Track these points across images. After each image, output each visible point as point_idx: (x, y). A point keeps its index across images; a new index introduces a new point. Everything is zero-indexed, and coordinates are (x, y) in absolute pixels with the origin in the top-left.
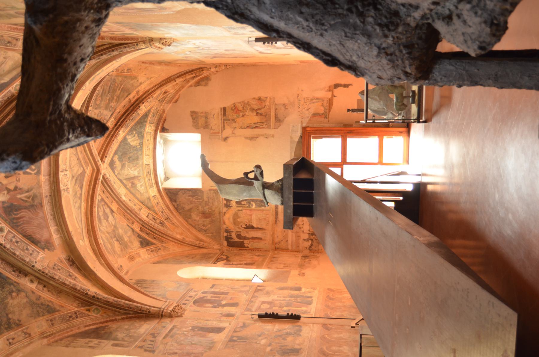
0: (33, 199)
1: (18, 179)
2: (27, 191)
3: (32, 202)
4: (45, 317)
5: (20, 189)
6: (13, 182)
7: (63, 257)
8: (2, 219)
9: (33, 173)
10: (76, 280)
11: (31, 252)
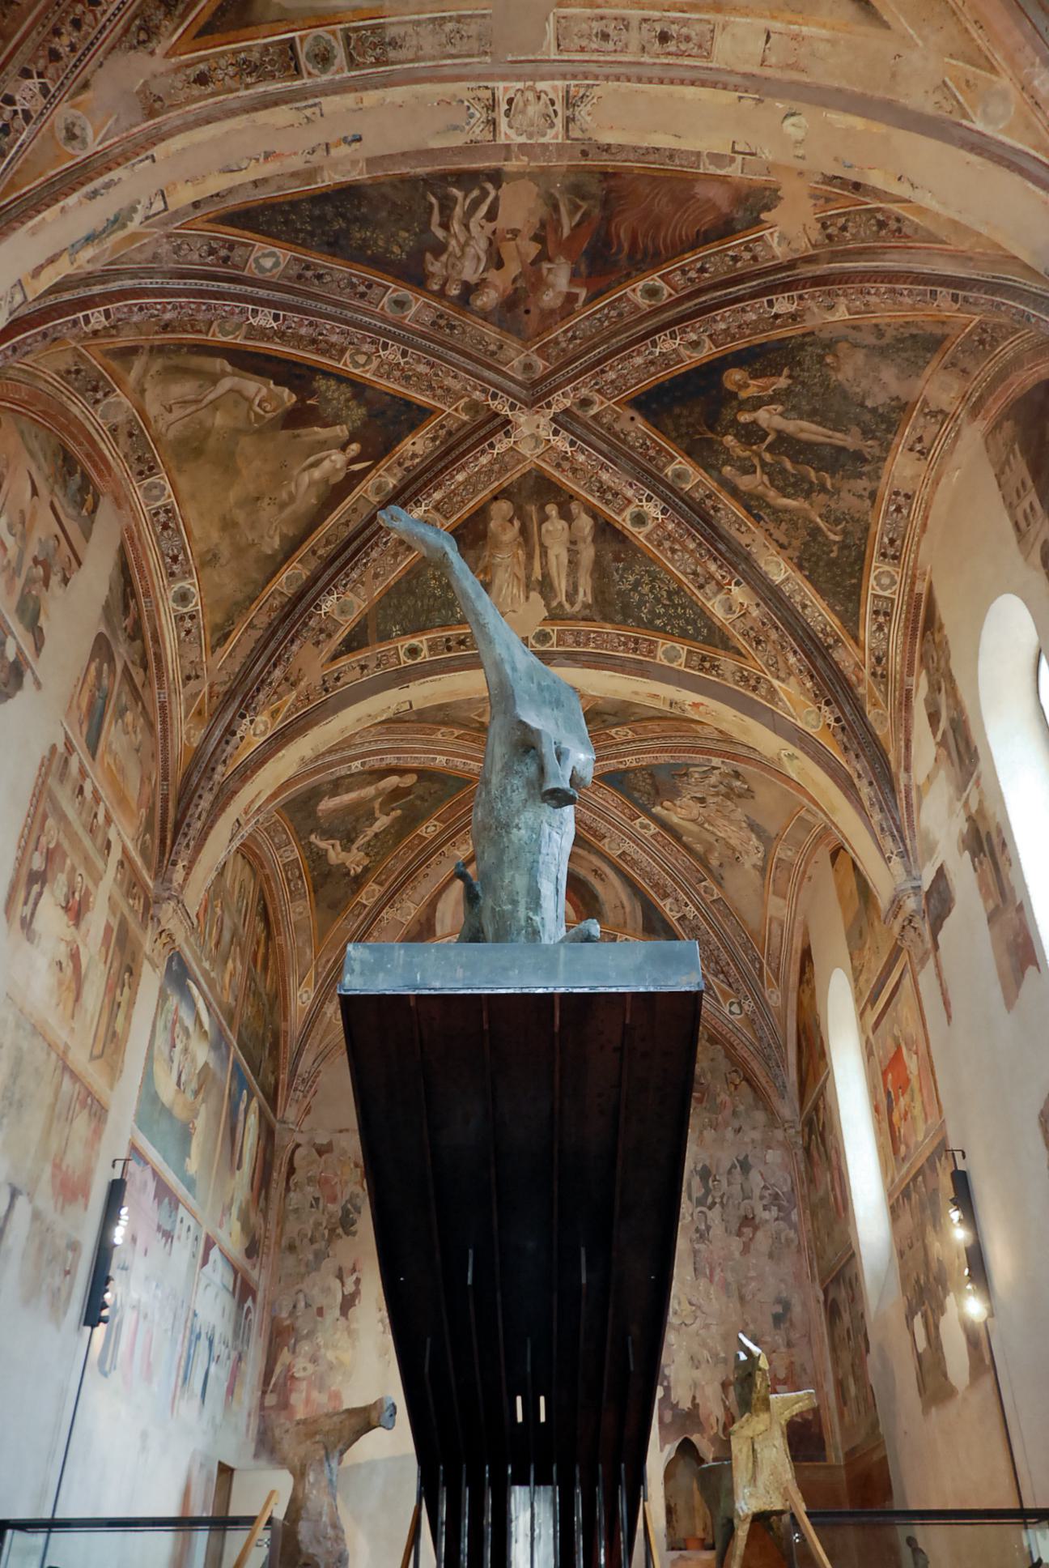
0: (583, 198)
1: (509, 236)
2: (556, 208)
3: (592, 202)
4: (934, 363)
5: (543, 225)
6: (517, 246)
7: (817, 183)
8: (620, 283)
9: (493, 193)
10: (906, 230)
11: (747, 255)
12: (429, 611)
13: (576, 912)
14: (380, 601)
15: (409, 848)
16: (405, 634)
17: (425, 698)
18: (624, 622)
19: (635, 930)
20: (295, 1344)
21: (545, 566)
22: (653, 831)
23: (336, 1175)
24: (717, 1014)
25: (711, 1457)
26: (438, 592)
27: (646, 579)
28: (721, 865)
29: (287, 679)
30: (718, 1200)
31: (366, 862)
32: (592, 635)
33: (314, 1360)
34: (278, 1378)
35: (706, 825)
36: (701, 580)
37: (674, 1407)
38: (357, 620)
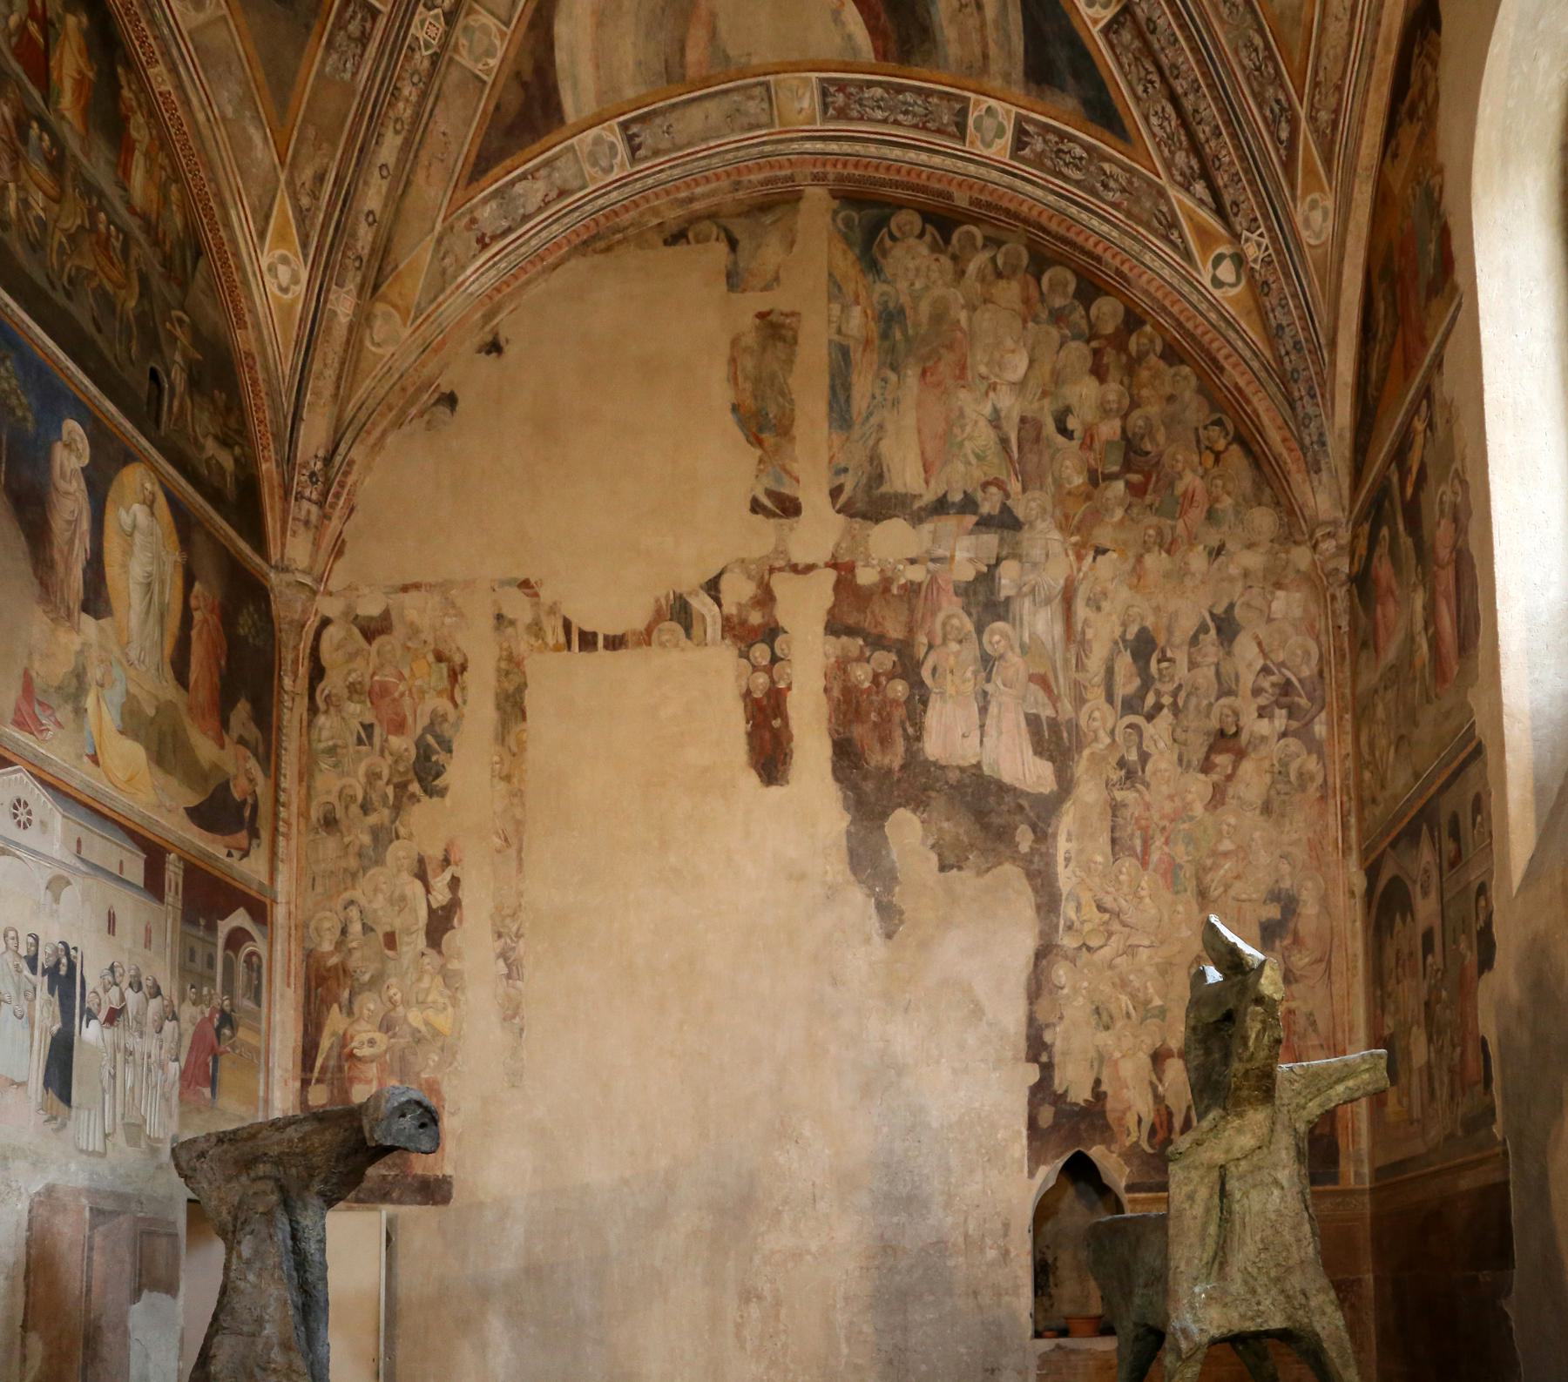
20: (350, 1002)
23: (401, 677)
25: (1123, 1184)
30: (1166, 700)
33: (387, 1026)
34: (327, 1058)
37: (1059, 1099)
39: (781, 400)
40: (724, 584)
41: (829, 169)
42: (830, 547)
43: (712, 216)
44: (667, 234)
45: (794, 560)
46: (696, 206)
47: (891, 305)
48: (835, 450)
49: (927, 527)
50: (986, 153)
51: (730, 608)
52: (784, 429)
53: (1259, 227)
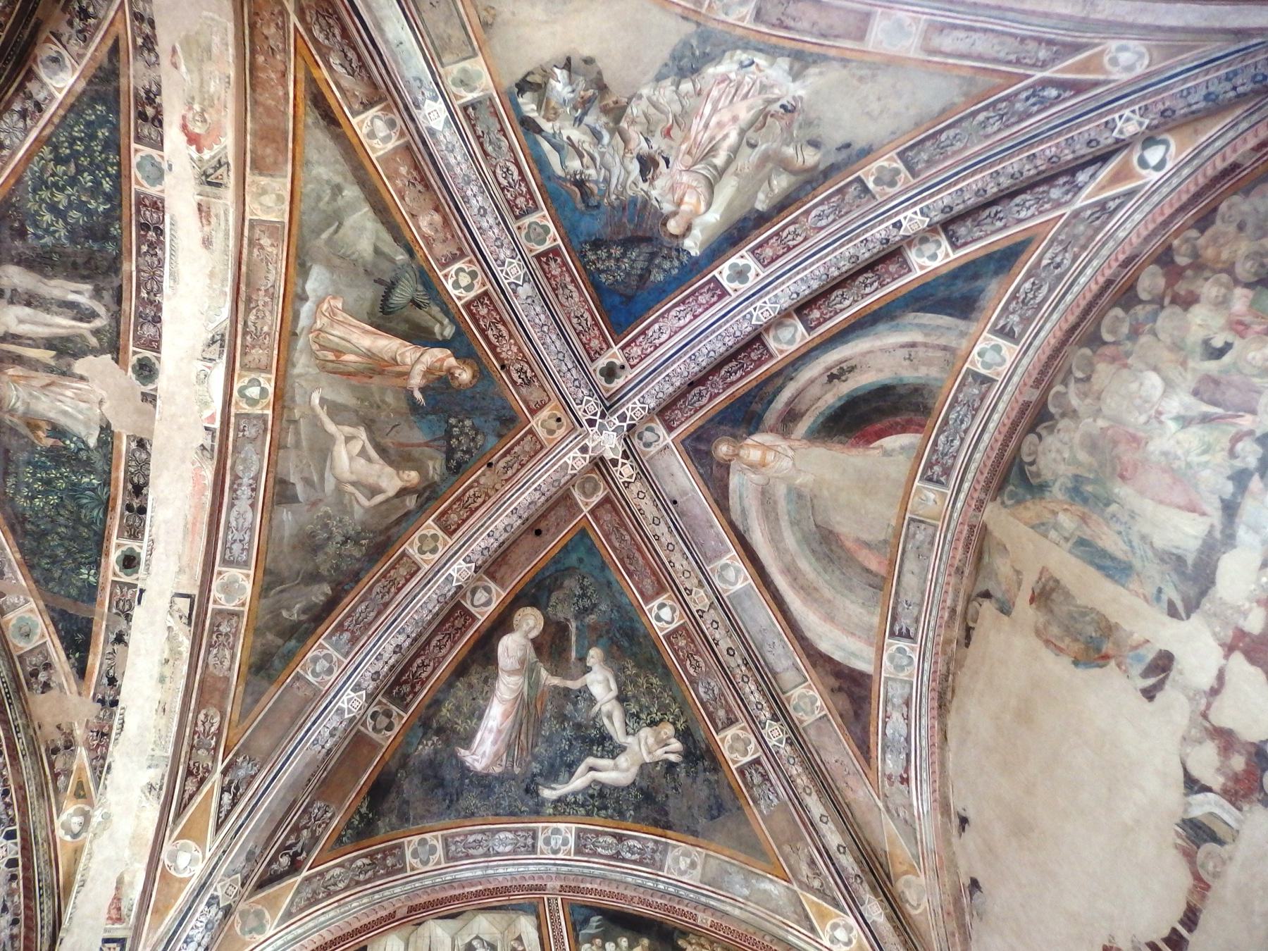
12: (78, 520)
13: (904, 430)
14: (36, 581)
15: (690, 656)
16: (98, 566)
17: (181, 571)
18: (117, 240)
19: (963, 334)
21: (35, 342)
22: (750, 261)
24: (1156, 199)
26: (54, 499)
27: (45, 194)
28: (815, 144)
29: (55, 751)
31: (667, 730)
32: (144, 295)
35: (719, 160)
36: (29, 105)
38: (48, 621)
39: (1088, 618)
40: (1195, 772)
41: (976, 495)
42: (1213, 644)
43: (969, 600)
44: (963, 641)
45: (1207, 688)
46: (959, 609)
47: (1070, 485)
48: (1141, 591)
49: (1242, 533)
50: (1008, 365)
51: (1217, 782)
52: (1108, 629)
53: (1114, 120)
